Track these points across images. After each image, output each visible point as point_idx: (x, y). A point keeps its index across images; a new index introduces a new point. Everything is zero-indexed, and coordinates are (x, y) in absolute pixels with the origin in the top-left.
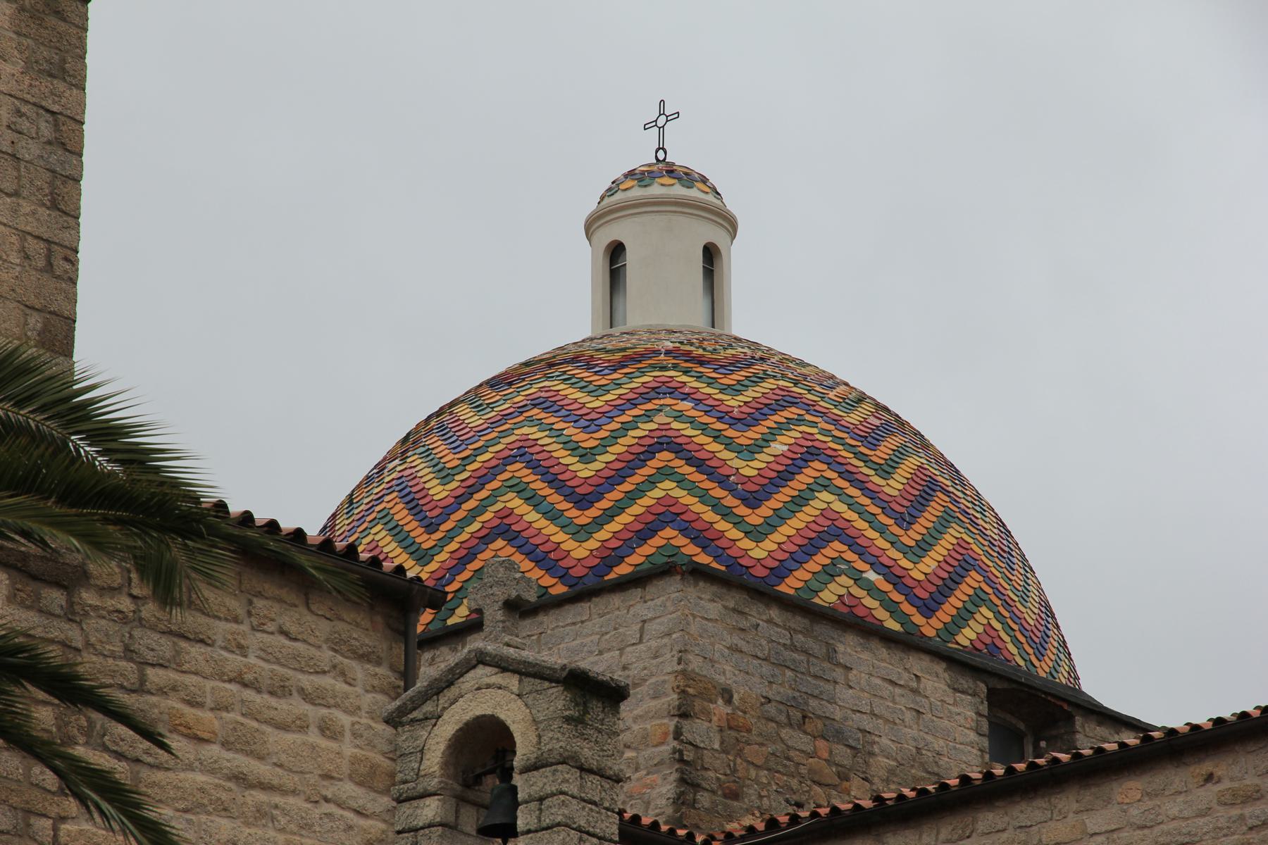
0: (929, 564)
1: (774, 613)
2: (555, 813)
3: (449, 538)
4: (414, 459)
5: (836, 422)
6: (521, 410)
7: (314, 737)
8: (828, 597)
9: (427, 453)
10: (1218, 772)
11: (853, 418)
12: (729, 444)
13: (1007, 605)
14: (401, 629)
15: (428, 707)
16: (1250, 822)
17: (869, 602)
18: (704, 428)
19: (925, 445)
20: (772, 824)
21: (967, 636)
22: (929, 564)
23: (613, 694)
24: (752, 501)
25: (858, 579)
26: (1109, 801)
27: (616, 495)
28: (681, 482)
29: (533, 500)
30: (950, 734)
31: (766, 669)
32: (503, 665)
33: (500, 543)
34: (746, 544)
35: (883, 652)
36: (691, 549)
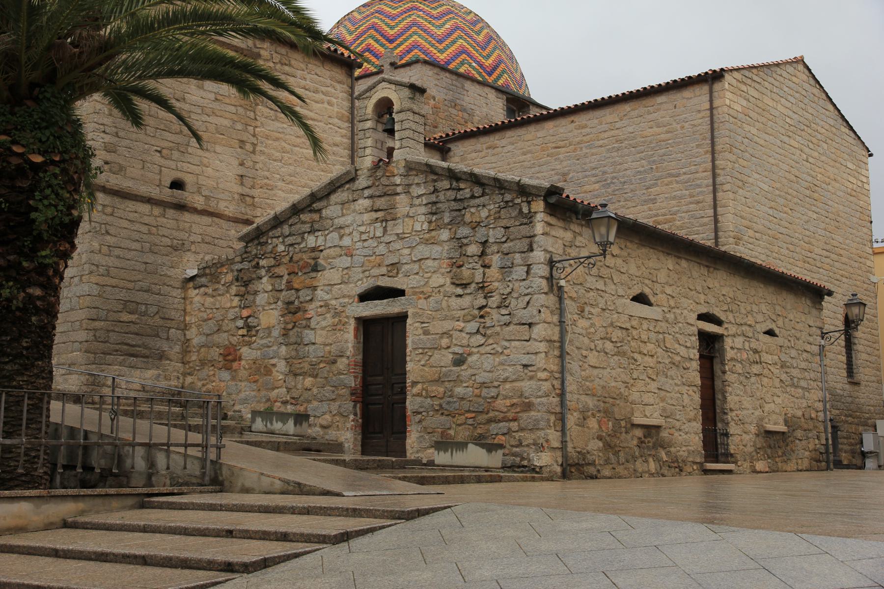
0: (490, 61)
1: (447, 74)
2: (406, 125)
4: (341, 28)
5: (464, 19)
6: (372, 14)
7: (326, 105)
8: (462, 70)
9: (345, 27)
11: (469, 18)
14: (351, 75)
15: (368, 94)
17: (473, 72)
18: (426, 20)
19: (489, 27)
20: (447, 135)
21: (500, 82)
22: (490, 61)
23: (422, 91)
24: (440, 42)
25: (470, 66)
27: (401, 40)
29: (377, 41)
30: (495, 110)
31: (445, 91)
32: (390, 82)
34: (438, 54)
35: (478, 87)
36: (423, 56)
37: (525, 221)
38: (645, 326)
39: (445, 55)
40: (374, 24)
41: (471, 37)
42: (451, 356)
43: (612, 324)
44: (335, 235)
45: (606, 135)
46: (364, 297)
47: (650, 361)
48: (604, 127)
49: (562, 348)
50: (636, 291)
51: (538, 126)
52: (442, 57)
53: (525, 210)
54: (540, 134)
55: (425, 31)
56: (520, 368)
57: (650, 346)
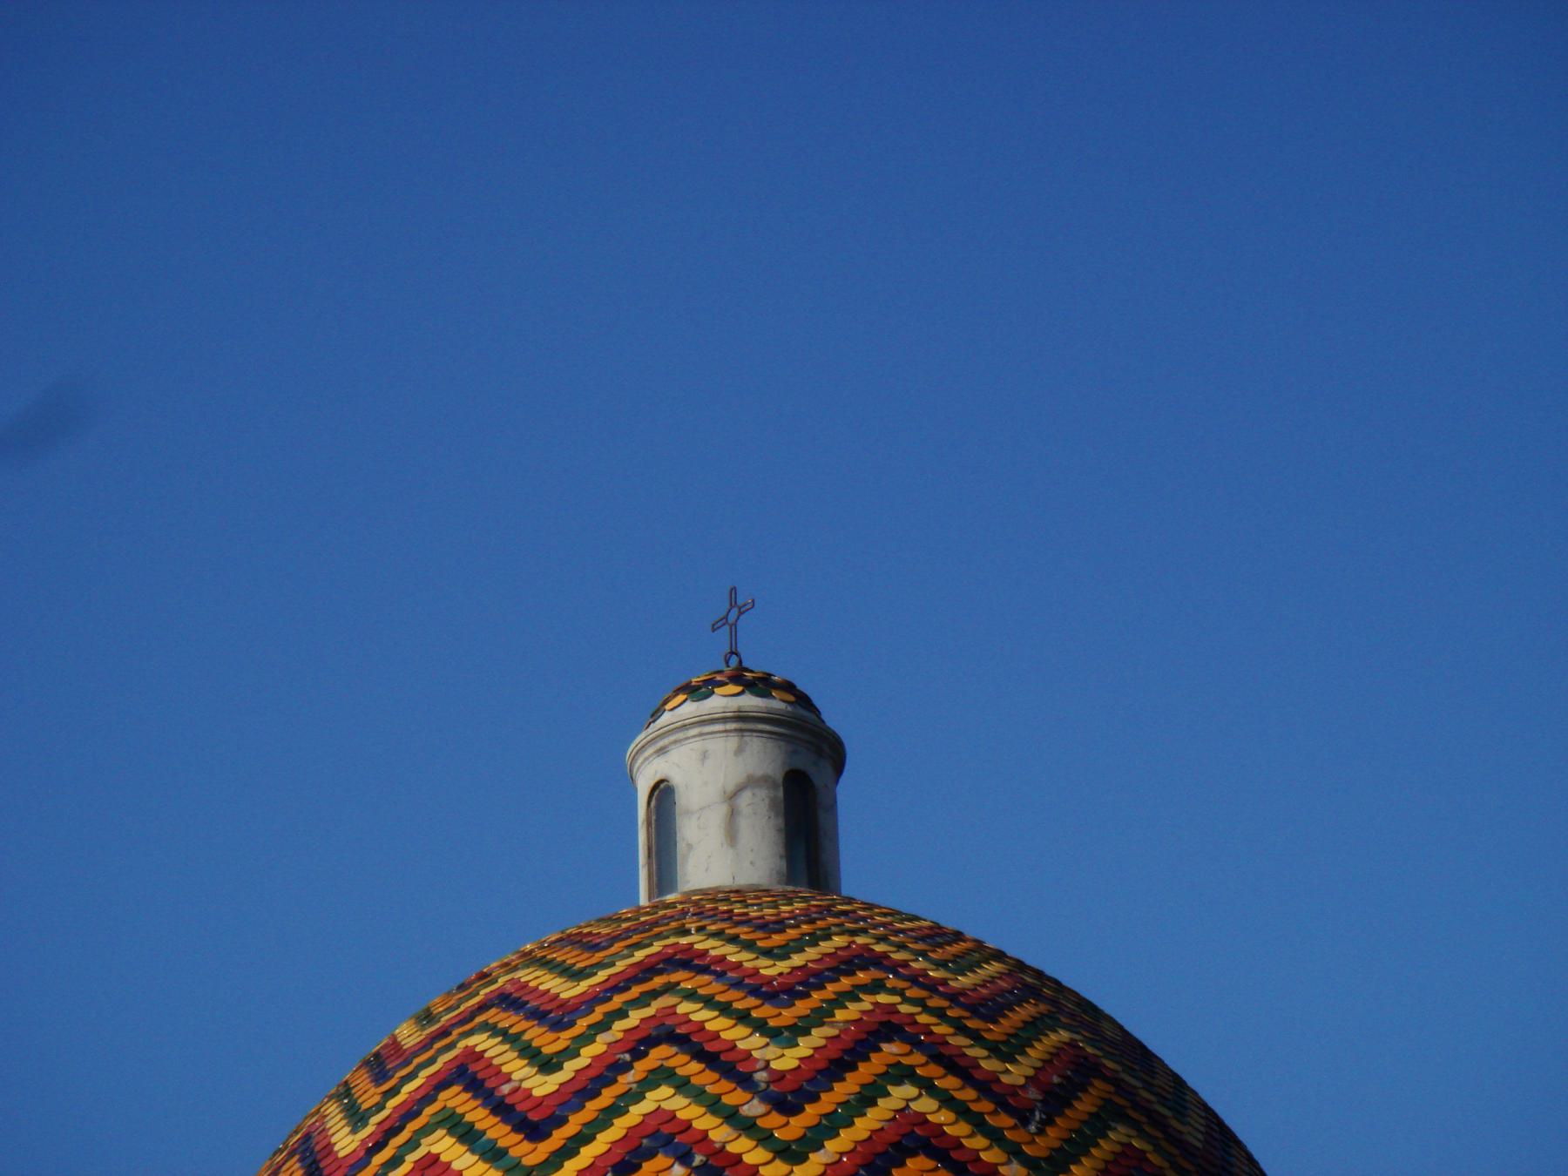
11: (964, 981)
12: (760, 1027)
18: (725, 1009)
28: (683, 1085)
40: (475, 1056)
55: (710, 1059)
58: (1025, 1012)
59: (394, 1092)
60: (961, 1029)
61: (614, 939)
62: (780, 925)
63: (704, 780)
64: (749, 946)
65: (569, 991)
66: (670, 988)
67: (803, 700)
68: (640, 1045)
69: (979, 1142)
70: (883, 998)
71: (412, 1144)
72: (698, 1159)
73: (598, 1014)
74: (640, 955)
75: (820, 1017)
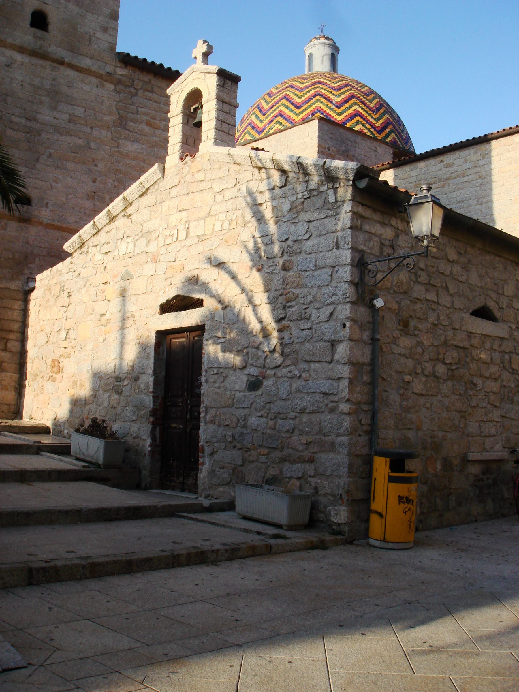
3: (267, 117)
8: (356, 129)
10: (444, 160)
11: (363, 90)
12: (334, 94)
13: (399, 133)
16: (451, 172)
18: (328, 91)
21: (388, 139)
26: (417, 168)
29: (287, 107)
33: (279, 117)
34: (337, 117)
35: (368, 141)
37: (330, 213)
38: (488, 345)
39: (343, 116)
41: (363, 103)
42: (245, 379)
43: (445, 342)
44: (143, 241)
45: (470, 172)
46: (167, 308)
47: (494, 386)
48: (469, 165)
49: (373, 372)
50: (478, 303)
51: (413, 166)
52: (339, 119)
53: (332, 199)
54: (414, 173)
56: (319, 397)
57: (494, 369)
58: (373, 95)
59: (273, 99)
60: (364, 97)
61: (308, 78)
62: (334, 78)
63: (318, 53)
64: (330, 81)
65: (302, 86)
66: (318, 87)
67: (334, 42)
68: (315, 96)
69: (367, 115)
70: (352, 92)
71: (278, 108)
72: (324, 114)
73: (307, 90)
74: (313, 81)
75: (343, 94)
